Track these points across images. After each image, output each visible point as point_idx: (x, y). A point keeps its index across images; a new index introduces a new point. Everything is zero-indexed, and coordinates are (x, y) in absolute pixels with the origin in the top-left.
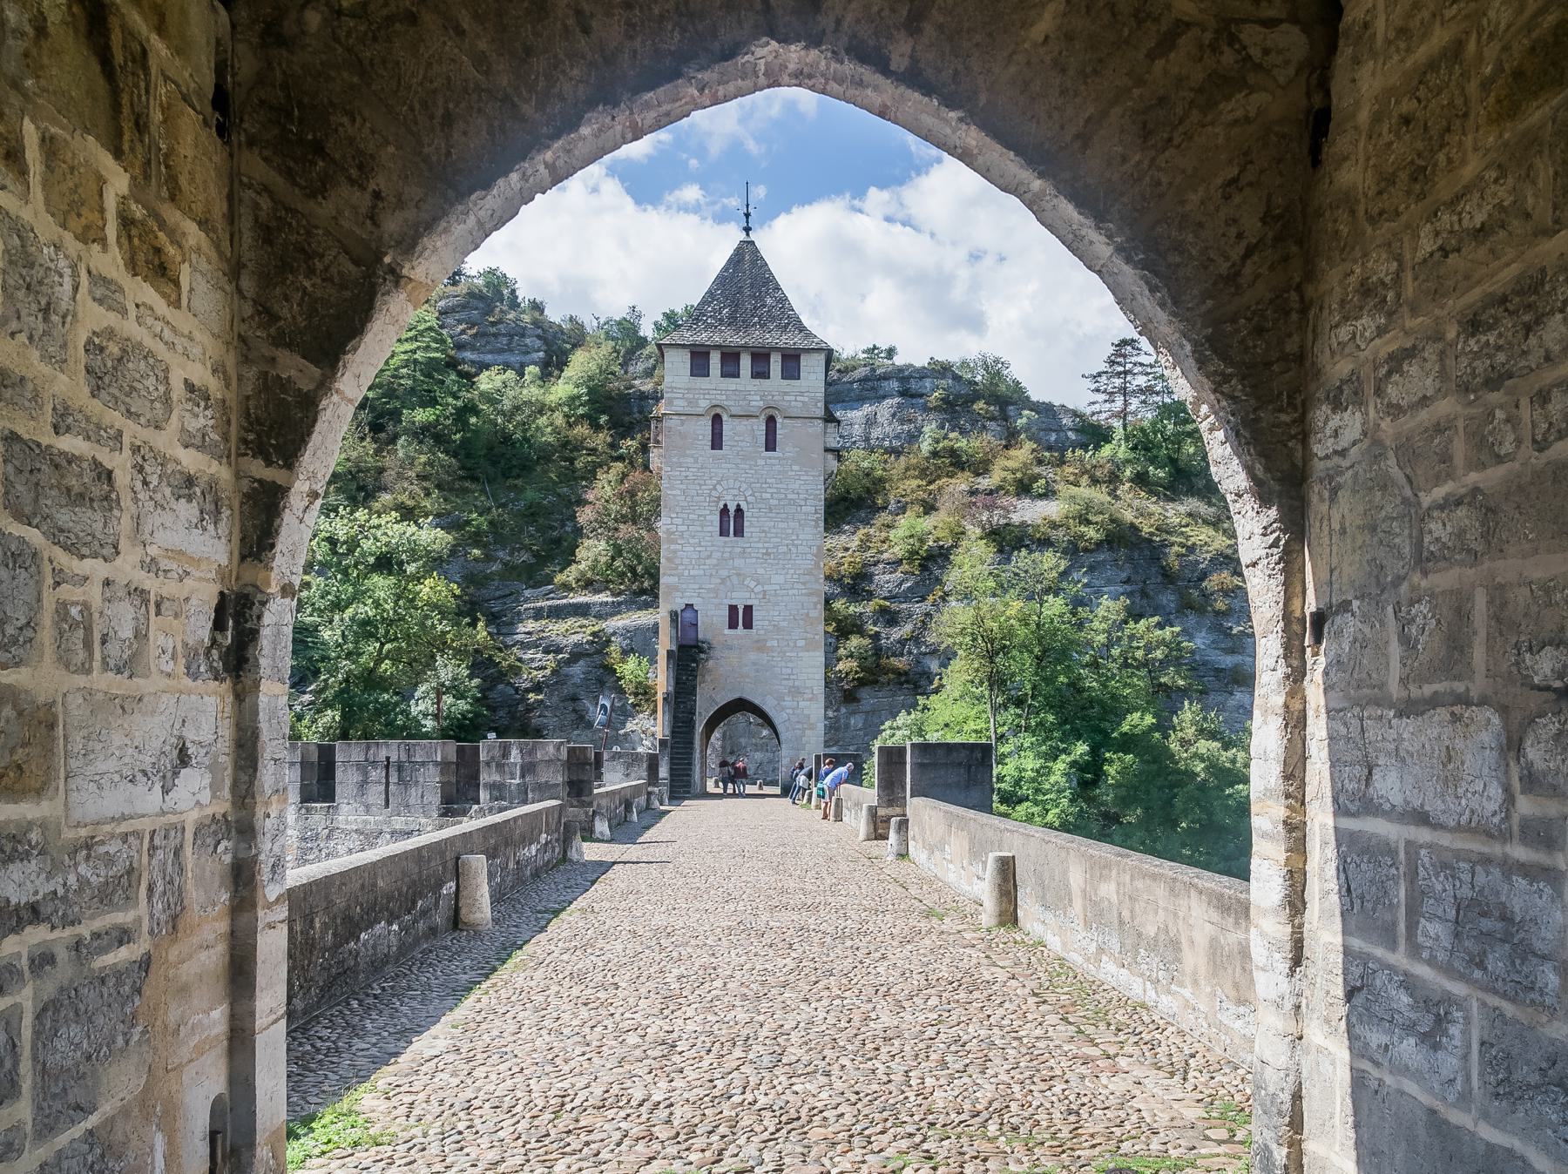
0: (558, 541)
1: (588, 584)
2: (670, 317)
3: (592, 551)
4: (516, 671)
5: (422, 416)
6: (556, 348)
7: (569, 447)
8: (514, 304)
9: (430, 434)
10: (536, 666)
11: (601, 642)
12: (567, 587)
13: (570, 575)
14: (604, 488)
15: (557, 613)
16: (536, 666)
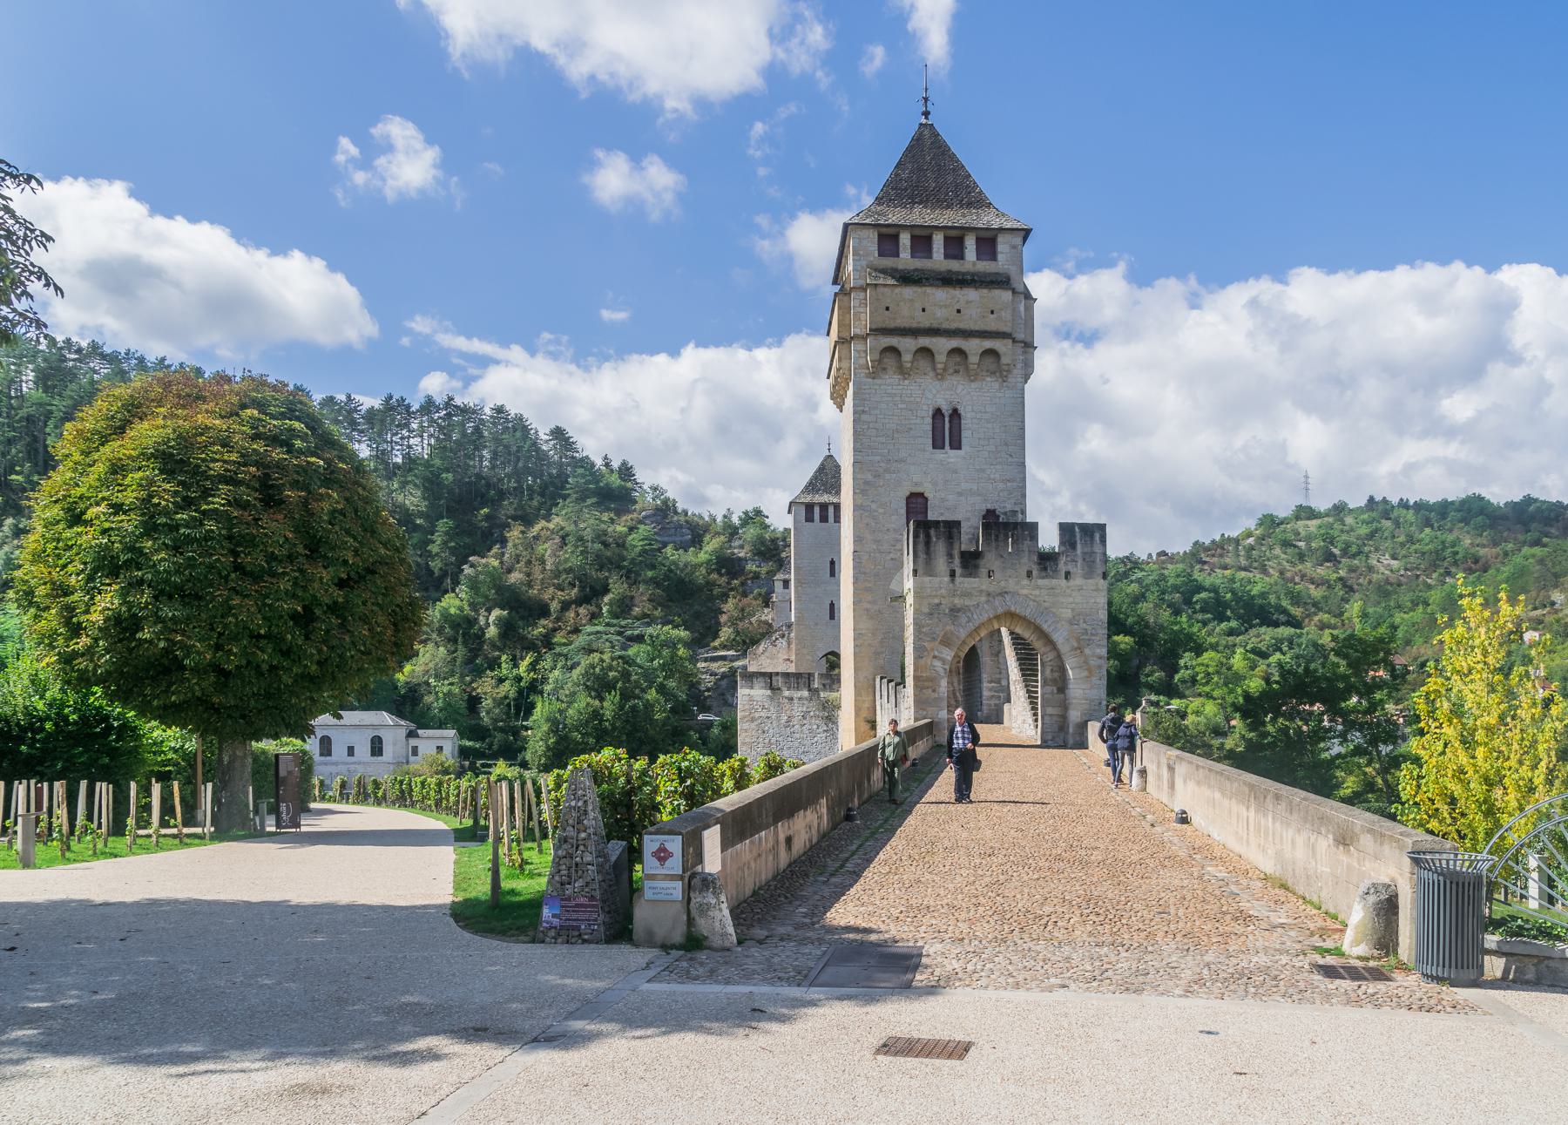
0: (709, 628)
1: (724, 647)
2: (746, 513)
3: (726, 633)
4: (699, 683)
5: (650, 574)
6: (696, 532)
7: (710, 585)
8: (676, 513)
9: (655, 582)
10: (708, 681)
11: (733, 672)
12: (715, 649)
13: (716, 643)
14: (730, 606)
15: (714, 659)
16: (708, 681)
